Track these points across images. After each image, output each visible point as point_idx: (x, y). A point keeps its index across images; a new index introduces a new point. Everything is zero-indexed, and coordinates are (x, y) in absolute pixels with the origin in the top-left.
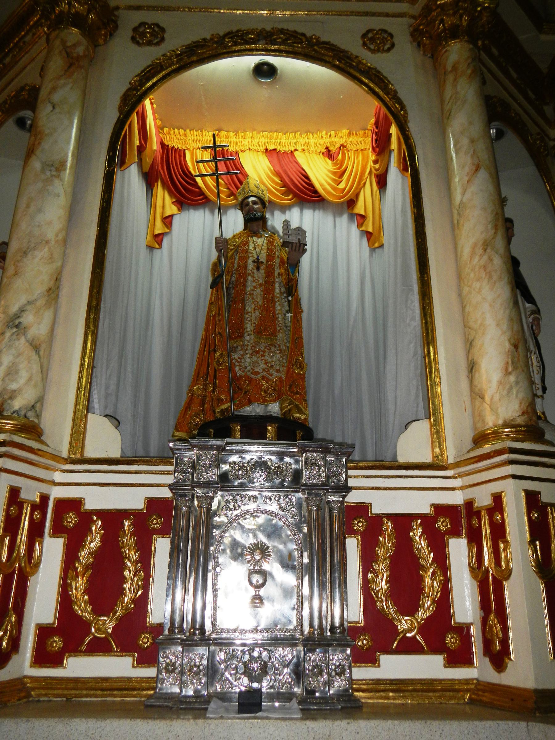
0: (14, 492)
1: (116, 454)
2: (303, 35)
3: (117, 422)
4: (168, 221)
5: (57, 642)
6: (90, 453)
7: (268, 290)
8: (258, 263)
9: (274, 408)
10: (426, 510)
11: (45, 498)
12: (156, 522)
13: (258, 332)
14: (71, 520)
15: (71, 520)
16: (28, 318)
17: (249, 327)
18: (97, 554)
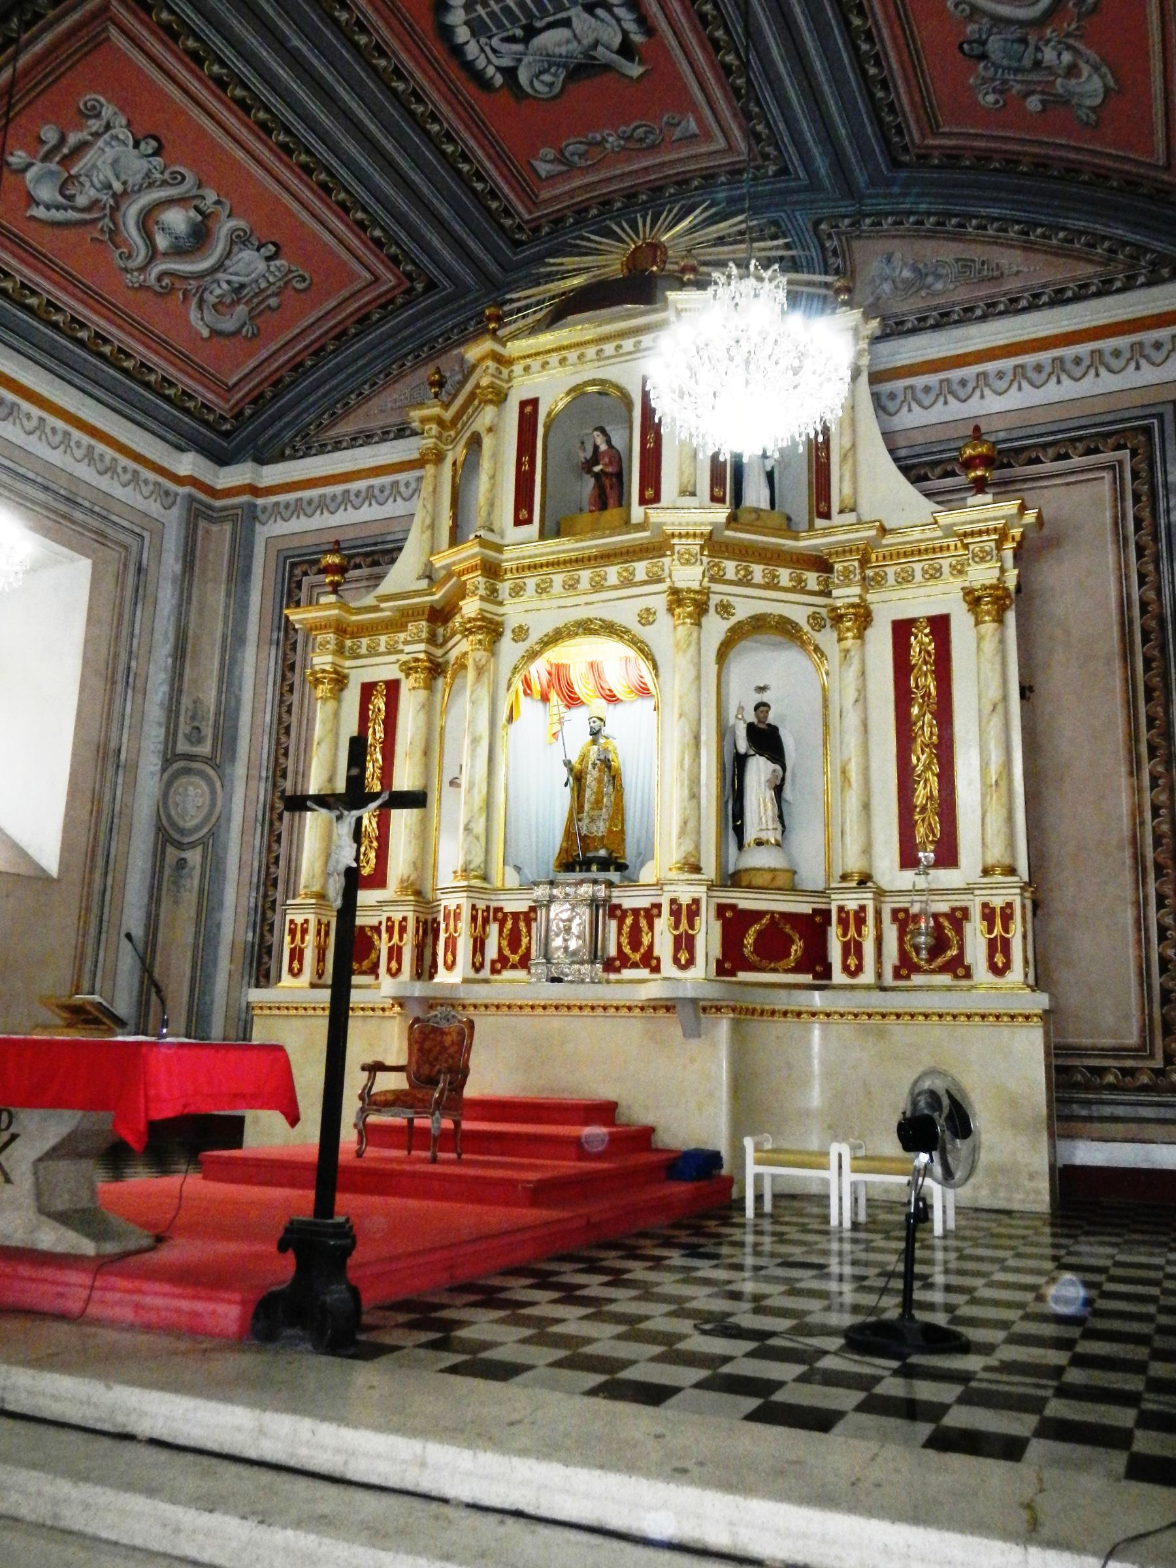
0: (474, 907)
1: (516, 886)
2: (603, 621)
3: (518, 869)
4: (561, 721)
5: (499, 966)
6: (508, 886)
7: (600, 781)
8: (594, 765)
9: (602, 853)
10: (647, 905)
11: (488, 907)
12: (532, 915)
13: (592, 809)
14: (500, 915)
15: (500, 915)
16: (473, 825)
17: (587, 807)
18: (512, 930)
